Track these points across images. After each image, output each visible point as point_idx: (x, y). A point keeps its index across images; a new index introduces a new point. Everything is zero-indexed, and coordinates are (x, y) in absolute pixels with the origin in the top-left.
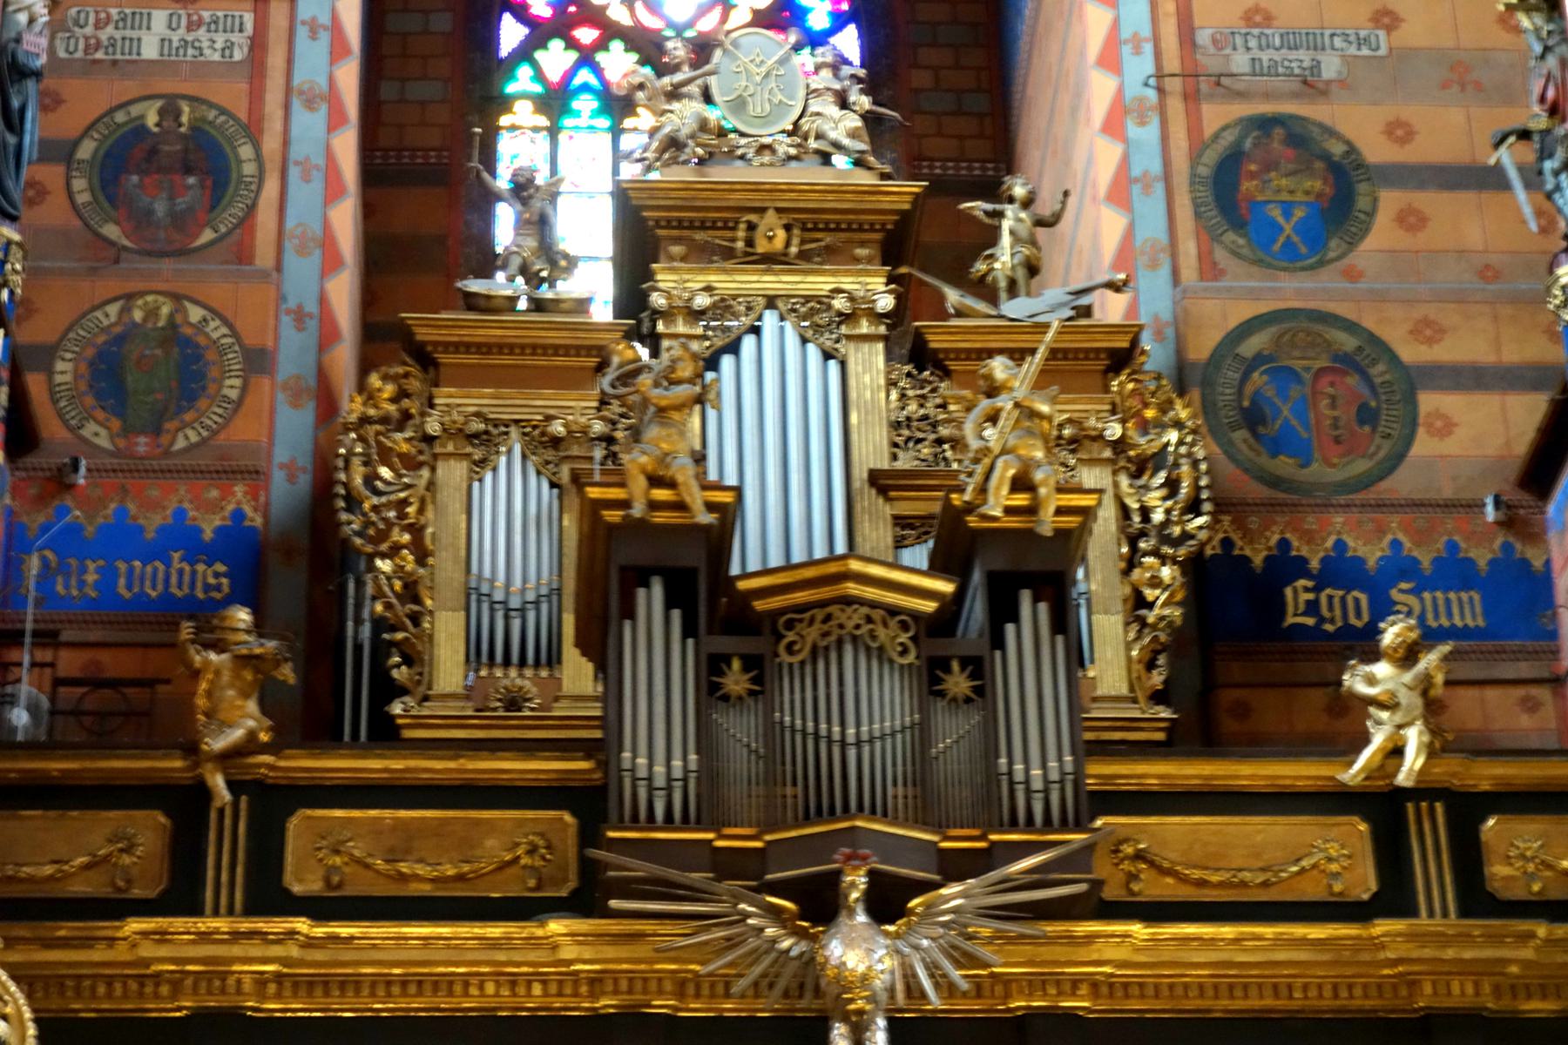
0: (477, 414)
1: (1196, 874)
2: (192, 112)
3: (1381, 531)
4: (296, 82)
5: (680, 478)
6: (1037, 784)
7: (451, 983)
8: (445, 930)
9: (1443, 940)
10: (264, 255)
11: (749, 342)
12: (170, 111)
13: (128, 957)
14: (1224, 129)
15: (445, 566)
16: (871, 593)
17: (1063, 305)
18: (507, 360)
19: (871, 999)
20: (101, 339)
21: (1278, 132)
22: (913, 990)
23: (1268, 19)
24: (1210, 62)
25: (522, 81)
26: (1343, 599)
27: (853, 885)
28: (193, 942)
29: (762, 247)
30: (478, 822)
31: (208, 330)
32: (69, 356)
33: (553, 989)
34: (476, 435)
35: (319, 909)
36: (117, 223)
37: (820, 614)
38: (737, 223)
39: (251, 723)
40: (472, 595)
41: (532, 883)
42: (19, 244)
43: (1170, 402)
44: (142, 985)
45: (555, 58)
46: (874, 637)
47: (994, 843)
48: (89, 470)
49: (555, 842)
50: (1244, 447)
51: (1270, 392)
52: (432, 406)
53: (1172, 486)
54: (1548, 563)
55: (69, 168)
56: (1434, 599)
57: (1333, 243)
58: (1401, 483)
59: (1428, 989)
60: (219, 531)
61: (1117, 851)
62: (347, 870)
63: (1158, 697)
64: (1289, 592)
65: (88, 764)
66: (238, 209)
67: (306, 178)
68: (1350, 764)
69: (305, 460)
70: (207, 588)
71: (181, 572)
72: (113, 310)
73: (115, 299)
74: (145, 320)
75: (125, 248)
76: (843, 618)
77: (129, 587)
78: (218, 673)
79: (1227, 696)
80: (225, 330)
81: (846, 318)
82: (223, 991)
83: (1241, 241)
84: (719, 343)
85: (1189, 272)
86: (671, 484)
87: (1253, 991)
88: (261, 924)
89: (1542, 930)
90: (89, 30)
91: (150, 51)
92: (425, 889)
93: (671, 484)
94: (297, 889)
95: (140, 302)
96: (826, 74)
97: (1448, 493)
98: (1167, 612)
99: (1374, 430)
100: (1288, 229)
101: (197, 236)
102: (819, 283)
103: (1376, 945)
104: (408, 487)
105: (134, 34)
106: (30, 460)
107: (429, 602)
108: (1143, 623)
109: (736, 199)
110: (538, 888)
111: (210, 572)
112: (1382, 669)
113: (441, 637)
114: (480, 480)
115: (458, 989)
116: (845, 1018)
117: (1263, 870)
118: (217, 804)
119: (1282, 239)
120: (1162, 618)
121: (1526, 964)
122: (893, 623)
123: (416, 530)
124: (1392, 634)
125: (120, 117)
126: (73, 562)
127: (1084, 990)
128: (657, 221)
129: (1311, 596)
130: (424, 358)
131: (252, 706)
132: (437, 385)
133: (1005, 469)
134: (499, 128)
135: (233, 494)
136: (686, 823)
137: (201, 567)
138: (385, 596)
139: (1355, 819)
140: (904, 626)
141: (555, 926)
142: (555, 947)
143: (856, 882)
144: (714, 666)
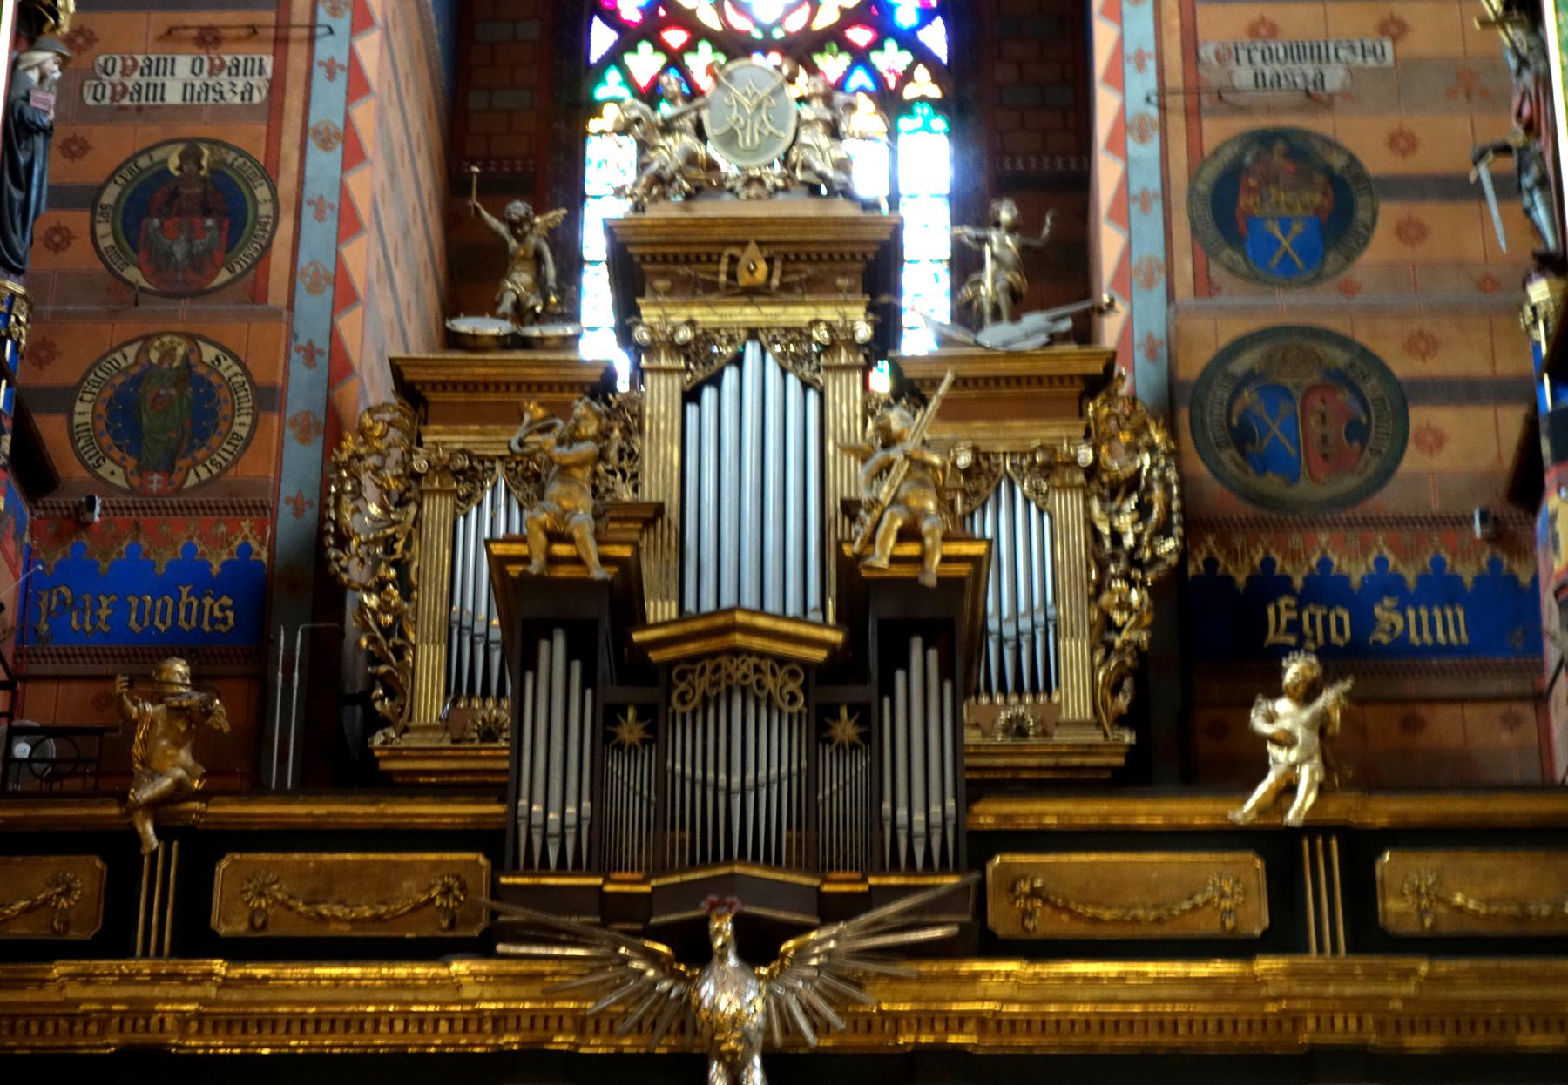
0: (463, 451)
1: (1090, 911)
2: (212, 153)
3: (1365, 549)
4: (312, 122)
5: (577, 534)
6: (919, 827)
7: (362, 1023)
8: (355, 971)
9: (1322, 977)
10: (277, 296)
11: (730, 375)
12: (191, 155)
13: (56, 997)
14: (1225, 144)
15: (429, 600)
16: (758, 643)
17: (1037, 332)
18: (493, 397)
19: (745, 1038)
20: (119, 381)
21: (1279, 146)
22: (789, 1026)
23: (1273, 32)
24: (1212, 76)
25: (610, 87)
26: (1326, 620)
27: (719, 931)
28: (115, 983)
29: (744, 279)
30: (396, 864)
31: (220, 369)
32: (88, 397)
33: (459, 1026)
34: (462, 471)
35: (237, 950)
36: (139, 267)
37: (709, 665)
38: (720, 255)
39: (180, 772)
40: (453, 629)
41: (445, 923)
42: (23, 297)
43: (1145, 426)
44: (72, 1025)
45: (645, 62)
46: (760, 684)
47: (871, 887)
48: (104, 508)
49: (470, 884)
50: (1233, 468)
51: (1260, 409)
52: (420, 444)
53: (1143, 510)
54: (1535, 579)
55: (93, 213)
56: (1418, 619)
57: (1331, 257)
58: (1390, 499)
59: (1311, 1024)
60: (224, 565)
61: (1013, 889)
62: (270, 912)
63: (1121, 721)
64: (1271, 611)
65: (31, 812)
66: (253, 250)
67: (320, 217)
68: (1245, 801)
69: (312, 494)
70: (213, 620)
71: (189, 606)
72: (131, 351)
73: (132, 342)
74: (161, 360)
75: (143, 290)
76: (732, 668)
77: (139, 620)
78: (153, 724)
80: (236, 369)
81: (827, 349)
82: (147, 1028)
83: (1238, 258)
84: (700, 376)
86: (568, 539)
87: (1138, 1027)
88: (182, 966)
89: (1423, 967)
90: (116, 77)
91: (173, 96)
92: (344, 929)
93: (568, 539)
94: (224, 930)
95: (157, 343)
96: (817, 104)
97: (1436, 507)
98: (1134, 636)
99: (1363, 443)
100: (1286, 244)
101: (213, 277)
102: (800, 314)
103: (1257, 981)
104: (394, 523)
105: (158, 80)
106: (47, 500)
107: (412, 636)
108: (1110, 647)
109: (719, 233)
110: (452, 926)
111: (216, 607)
112: (1284, 706)
113: (422, 671)
114: (466, 516)
115: (368, 1026)
116: (721, 1057)
117: (1156, 906)
118: (145, 850)
119: (1279, 253)
120: (1129, 642)
121: (1406, 1000)
122: (782, 673)
123: (401, 566)
124: (1293, 670)
125: (144, 162)
126: (87, 597)
127: (970, 1025)
128: (643, 258)
129: (1294, 615)
131: (184, 755)
132: (425, 423)
133: (893, 518)
134: (585, 134)
135: (241, 529)
136: (577, 869)
137: (208, 601)
138: (370, 629)
139: (1250, 856)
140: (793, 674)
141: (459, 967)
142: (459, 987)
143: (723, 929)
144: (608, 716)
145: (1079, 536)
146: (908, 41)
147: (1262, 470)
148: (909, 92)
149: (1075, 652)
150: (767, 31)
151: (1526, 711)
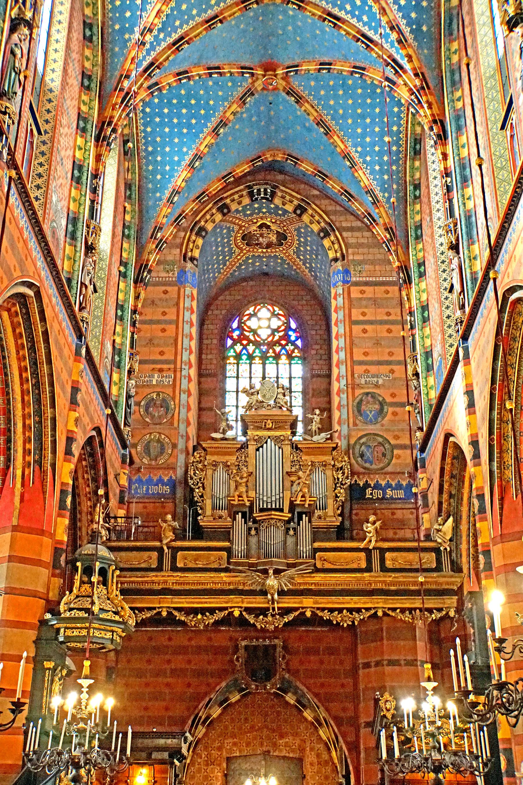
10: (176, 425)
11: (265, 445)
23: (369, 372)
24: (357, 381)
25: (231, 353)
29: (267, 426)
45: (238, 348)
53: (343, 473)
63: (339, 515)
79: (354, 512)
85: (351, 425)
91: (154, 382)
92: (201, 566)
102: (278, 433)
103: (364, 577)
112: (369, 525)
123: (203, 484)
130: (204, 449)
143: (271, 572)
144: (250, 529)
145: (332, 478)
146: (293, 343)
147: (366, 462)
148: (294, 355)
149: (330, 502)
150: (264, 340)
151: (414, 511)
